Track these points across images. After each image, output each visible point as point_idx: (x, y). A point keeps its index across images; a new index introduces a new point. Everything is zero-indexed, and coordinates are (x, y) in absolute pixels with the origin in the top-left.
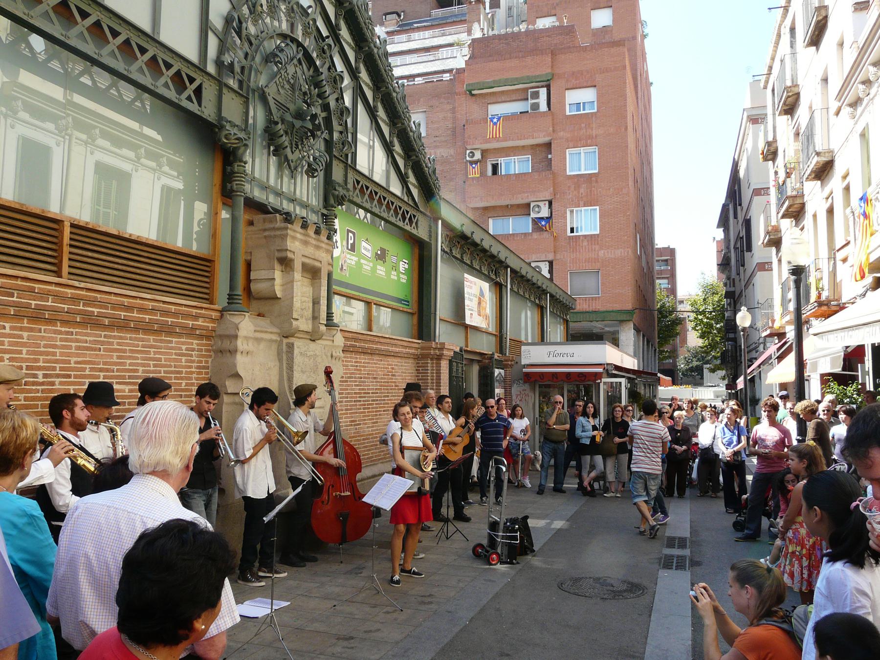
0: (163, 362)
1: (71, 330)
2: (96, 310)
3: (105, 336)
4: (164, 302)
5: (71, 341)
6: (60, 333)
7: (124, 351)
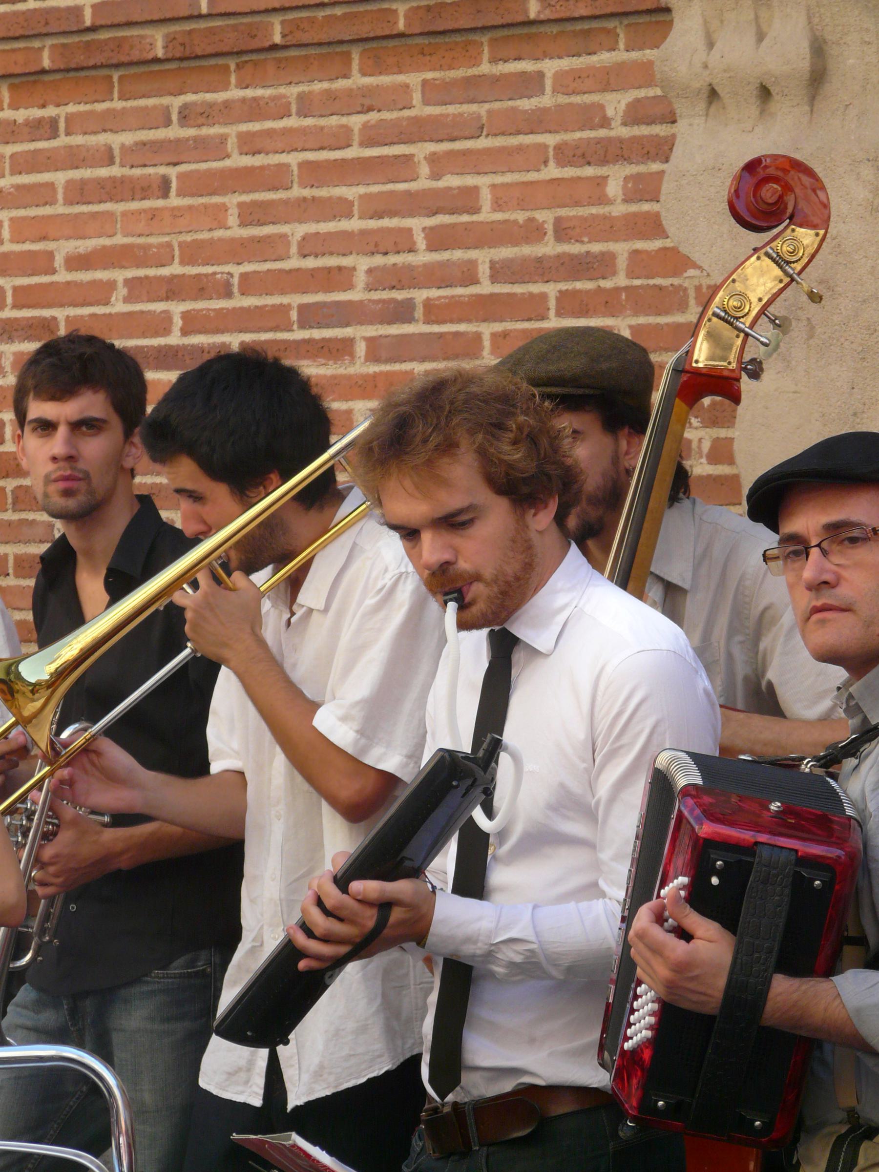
0: (487, 214)
1: (50, 111)
3: (186, 116)
5: (49, 161)
7: (276, 178)
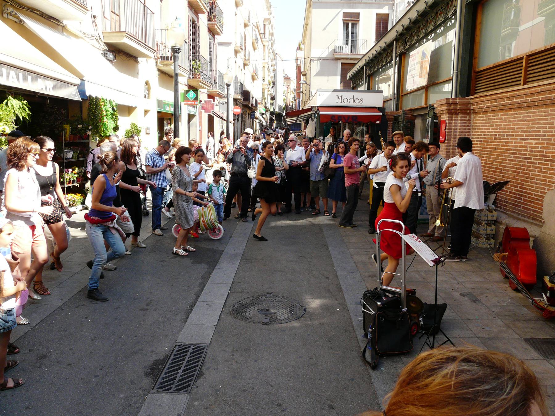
2: (519, 100)
4: (547, 85)
6: (512, 114)
